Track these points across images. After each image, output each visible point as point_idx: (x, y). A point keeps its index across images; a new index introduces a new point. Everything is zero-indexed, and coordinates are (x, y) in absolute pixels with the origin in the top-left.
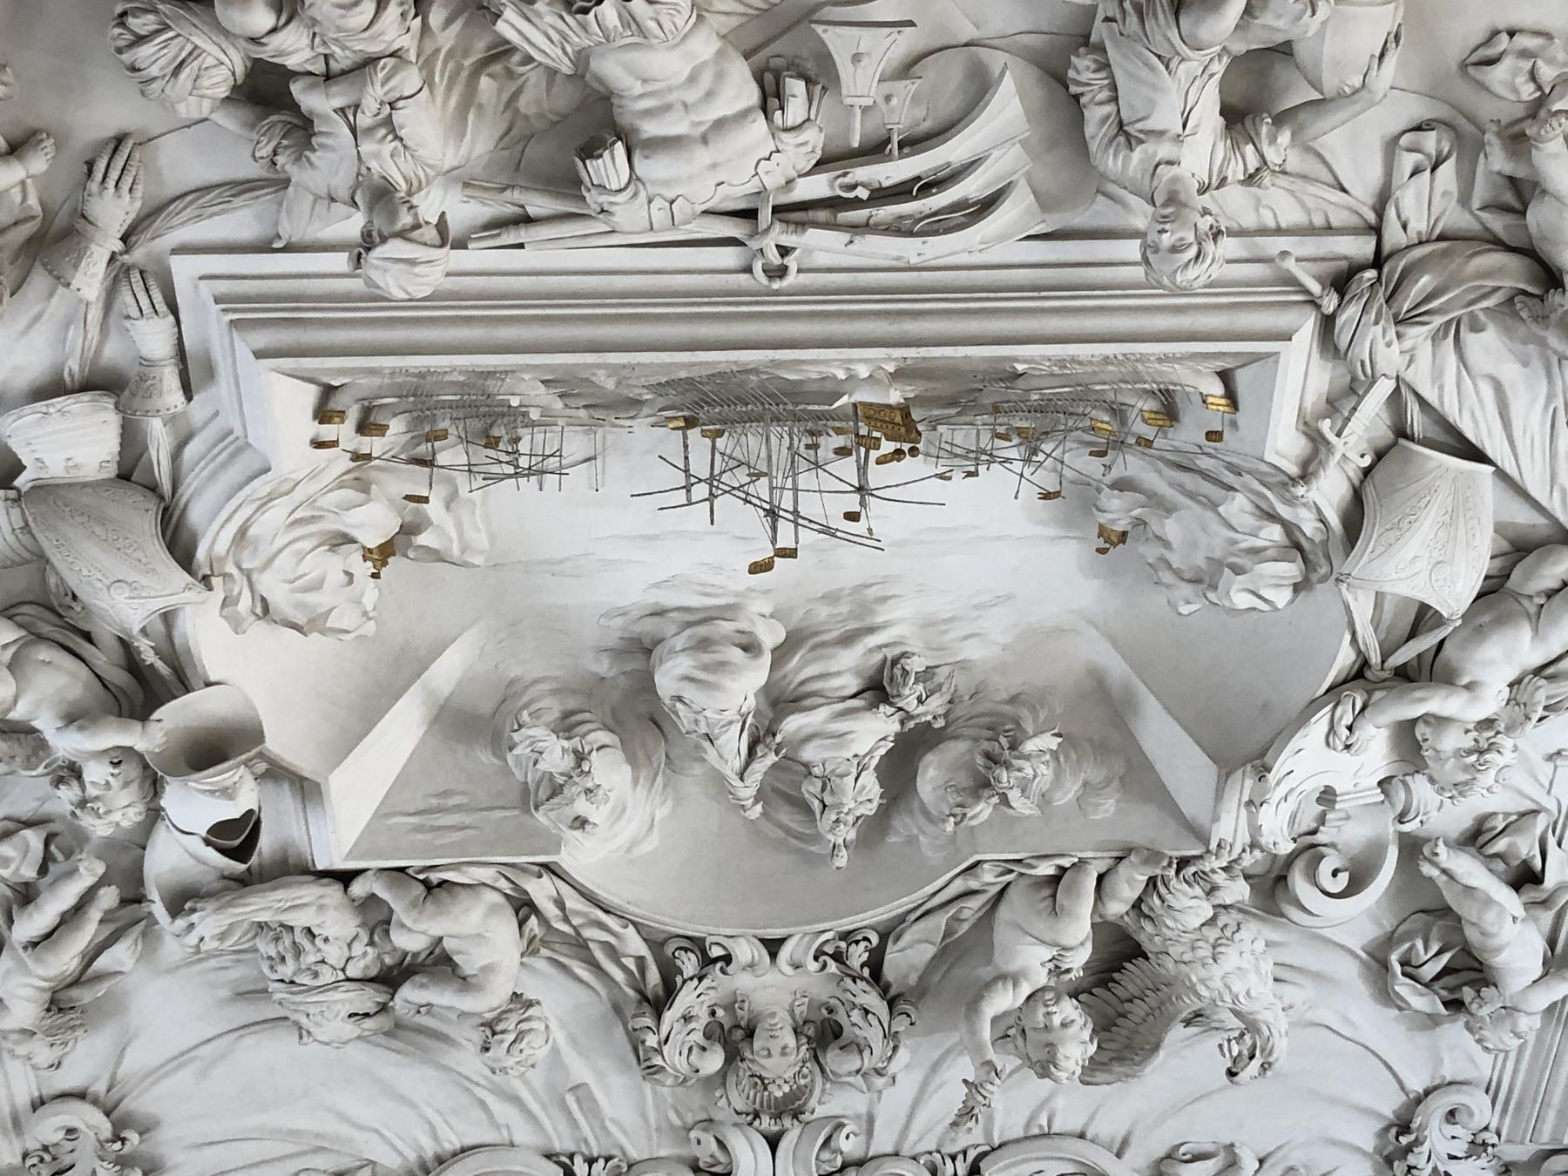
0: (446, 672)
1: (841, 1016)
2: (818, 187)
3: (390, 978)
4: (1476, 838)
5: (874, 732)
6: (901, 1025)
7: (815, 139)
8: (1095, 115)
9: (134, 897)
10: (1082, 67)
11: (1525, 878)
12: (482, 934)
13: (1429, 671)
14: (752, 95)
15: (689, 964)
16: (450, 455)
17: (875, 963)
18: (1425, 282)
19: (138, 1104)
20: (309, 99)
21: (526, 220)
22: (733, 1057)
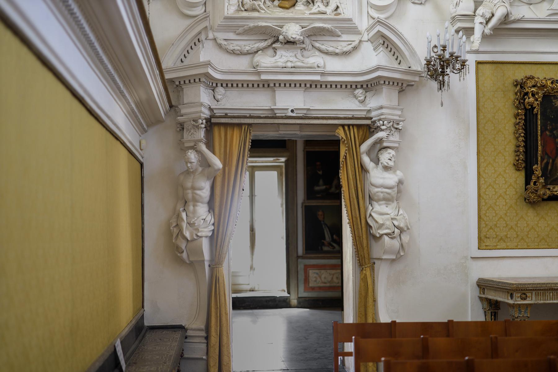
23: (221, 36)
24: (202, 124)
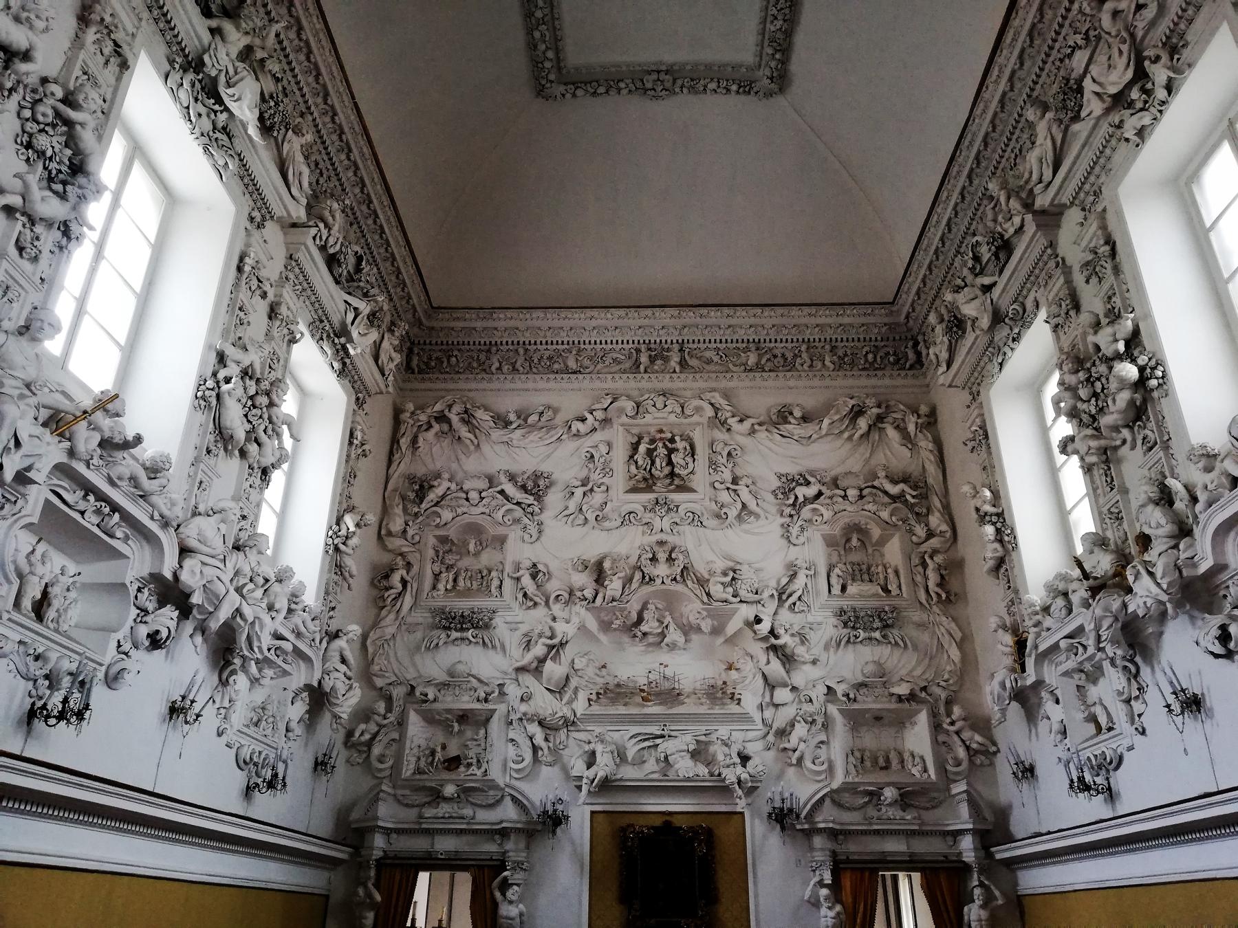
0: (721, 640)
2: (658, 741)
3: (733, 579)
4: (536, 604)
5: (644, 627)
7: (659, 750)
9: (780, 598)
10: (618, 760)
11: (525, 595)
12: (716, 590)
13: (551, 647)
15: (678, 578)
17: (644, 577)
19: (784, 542)
23: (399, 792)
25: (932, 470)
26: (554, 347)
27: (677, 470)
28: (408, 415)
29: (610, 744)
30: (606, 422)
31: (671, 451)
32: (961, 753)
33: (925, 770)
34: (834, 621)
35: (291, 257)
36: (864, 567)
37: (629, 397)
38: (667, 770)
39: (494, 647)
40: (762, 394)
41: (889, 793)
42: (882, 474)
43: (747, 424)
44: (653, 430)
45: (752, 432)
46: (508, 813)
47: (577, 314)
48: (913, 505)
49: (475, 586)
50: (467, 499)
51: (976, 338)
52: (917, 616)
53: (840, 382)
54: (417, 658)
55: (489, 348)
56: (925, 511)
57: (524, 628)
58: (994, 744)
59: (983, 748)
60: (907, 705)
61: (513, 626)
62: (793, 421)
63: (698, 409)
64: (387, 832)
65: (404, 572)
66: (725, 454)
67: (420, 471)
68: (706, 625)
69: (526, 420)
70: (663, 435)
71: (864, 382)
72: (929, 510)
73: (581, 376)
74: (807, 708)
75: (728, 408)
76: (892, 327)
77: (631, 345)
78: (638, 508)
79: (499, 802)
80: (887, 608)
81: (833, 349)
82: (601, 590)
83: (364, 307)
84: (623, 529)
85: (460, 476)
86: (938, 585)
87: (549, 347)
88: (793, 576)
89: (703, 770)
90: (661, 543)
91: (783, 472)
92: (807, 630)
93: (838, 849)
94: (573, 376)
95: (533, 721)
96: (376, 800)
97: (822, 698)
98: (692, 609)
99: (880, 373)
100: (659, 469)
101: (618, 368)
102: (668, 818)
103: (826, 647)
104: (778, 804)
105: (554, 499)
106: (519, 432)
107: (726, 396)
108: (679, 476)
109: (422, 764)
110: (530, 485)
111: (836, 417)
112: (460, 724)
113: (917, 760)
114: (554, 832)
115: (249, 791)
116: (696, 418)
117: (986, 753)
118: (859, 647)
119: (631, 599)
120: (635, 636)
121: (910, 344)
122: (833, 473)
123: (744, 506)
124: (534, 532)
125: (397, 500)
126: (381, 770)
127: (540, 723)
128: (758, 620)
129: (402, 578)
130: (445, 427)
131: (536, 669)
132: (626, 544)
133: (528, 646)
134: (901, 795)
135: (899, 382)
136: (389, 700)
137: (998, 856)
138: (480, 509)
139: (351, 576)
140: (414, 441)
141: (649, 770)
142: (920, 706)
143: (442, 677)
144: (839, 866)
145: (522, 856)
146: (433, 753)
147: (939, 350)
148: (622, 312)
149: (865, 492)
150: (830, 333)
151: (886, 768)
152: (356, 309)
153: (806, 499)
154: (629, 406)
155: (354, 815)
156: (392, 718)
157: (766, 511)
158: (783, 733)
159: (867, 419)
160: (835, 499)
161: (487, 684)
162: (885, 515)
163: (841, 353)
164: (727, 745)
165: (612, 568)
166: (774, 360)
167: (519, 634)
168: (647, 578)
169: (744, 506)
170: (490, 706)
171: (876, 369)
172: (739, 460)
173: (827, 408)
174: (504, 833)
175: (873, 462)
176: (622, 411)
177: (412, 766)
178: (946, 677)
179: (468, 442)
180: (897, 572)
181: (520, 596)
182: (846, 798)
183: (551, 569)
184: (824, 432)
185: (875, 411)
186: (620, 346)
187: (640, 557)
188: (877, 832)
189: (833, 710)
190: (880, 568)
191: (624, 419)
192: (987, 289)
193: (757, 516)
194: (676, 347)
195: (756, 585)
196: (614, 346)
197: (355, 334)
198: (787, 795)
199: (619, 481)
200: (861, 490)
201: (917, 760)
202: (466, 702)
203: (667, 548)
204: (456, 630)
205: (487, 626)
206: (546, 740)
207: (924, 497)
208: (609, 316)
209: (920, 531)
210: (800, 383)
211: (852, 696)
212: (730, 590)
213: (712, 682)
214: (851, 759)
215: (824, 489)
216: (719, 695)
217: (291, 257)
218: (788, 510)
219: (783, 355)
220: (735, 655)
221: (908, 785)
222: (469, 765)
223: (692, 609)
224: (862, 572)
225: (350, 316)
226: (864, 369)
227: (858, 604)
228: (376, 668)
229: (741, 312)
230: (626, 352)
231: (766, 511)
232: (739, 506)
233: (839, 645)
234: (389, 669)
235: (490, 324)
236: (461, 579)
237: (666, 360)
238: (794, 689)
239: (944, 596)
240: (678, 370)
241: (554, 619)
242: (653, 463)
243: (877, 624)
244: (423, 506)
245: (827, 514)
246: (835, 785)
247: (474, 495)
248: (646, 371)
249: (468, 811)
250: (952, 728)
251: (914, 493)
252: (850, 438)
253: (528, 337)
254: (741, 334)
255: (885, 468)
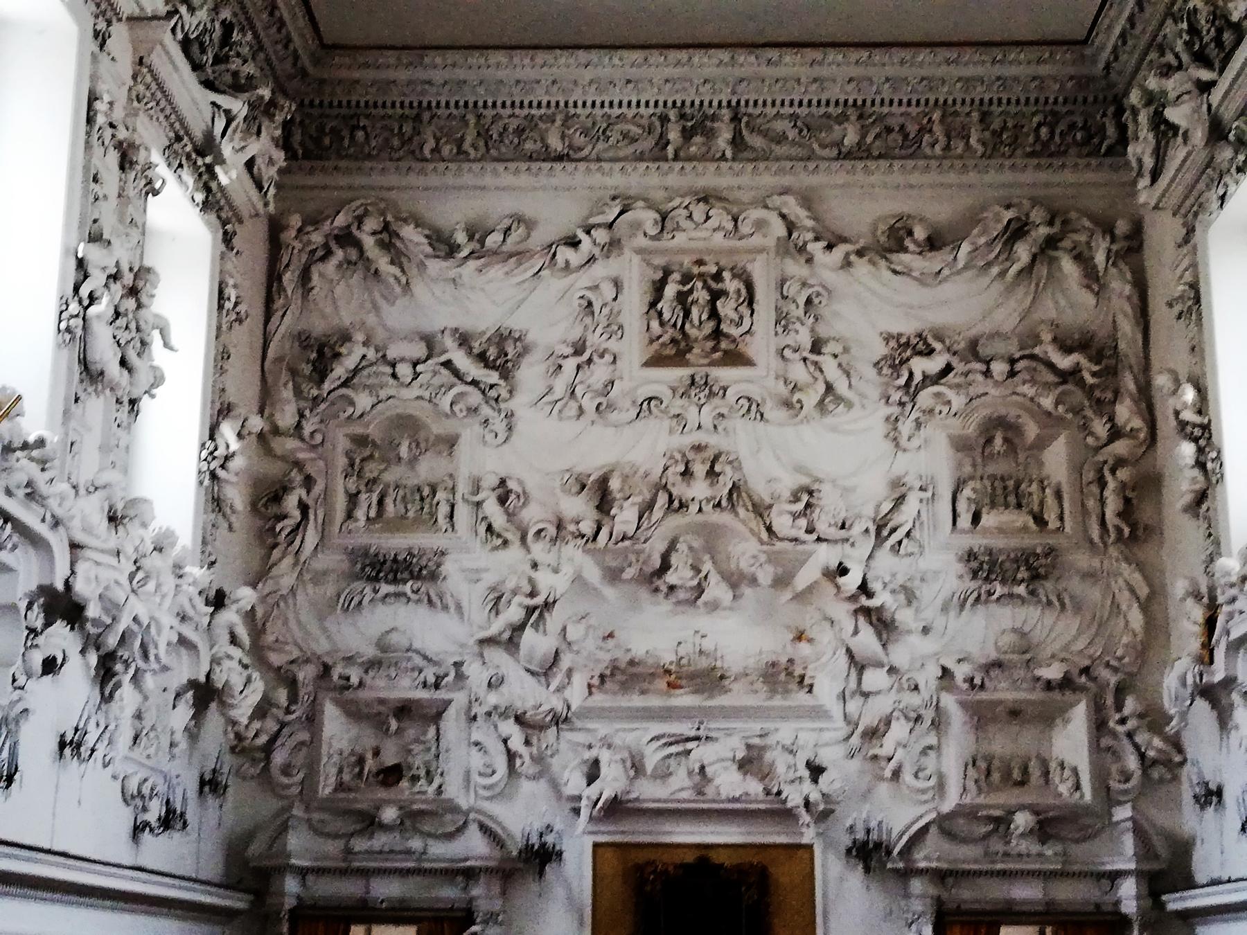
0: (787, 595)
1: (679, 478)
2: (690, 745)
3: (808, 505)
5: (671, 578)
6: (664, 481)
8: (629, 764)
10: (632, 773)
11: (490, 528)
12: (782, 523)
13: (530, 610)
14: (707, 769)
15: (724, 503)
16: (783, 660)
17: (671, 501)
18: (549, 718)
19: (888, 446)
20: (806, 773)
21: (761, 736)
22: (712, 467)
23: (316, 816)
24: (284, 915)
25: (1127, 328)
26: (526, 111)
27: (724, 327)
28: (293, 233)
29: (621, 746)
30: (614, 246)
31: (716, 295)
32: (1132, 763)
33: (1078, 787)
34: (960, 568)
35: (141, 61)
36: (1011, 483)
37: (650, 205)
38: (702, 787)
39: (445, 608)
40: (866, 198)
41: (1022, 820)
42: (1047, 337)
43: (840, 251)
44: (687, 261)
45: (847, 264)
46: (473, 846)
47: (564, 58)
48: (1092, 387)
49: (411, 514)
50: (394, 376)
51: (1189, 154)
52: (1083, 560)
53: (992, 177)
54: (330, 624)
55: (418, 114)
56: (1109, 395)
57: (489, 579)
58: (1180, 750)
59: (1163, 757)
60: (1056, 695)
61: (475, 577)
62: (912, 247)
63: (760, 225)
64: (303, 873)
65: (303, 492)
66: (801, 301)
67: (318, 327)
68: (765, 576)
69: (482, 242)
70: (703, 269)
71: (1028, 177)
72: (1117, 393)
73: (570, 166)
74: (914, 700)
75: (810, 223)
76: (1083, 82)
77: (651, 110)
78: (665, 393)
79: (460, 830)
80: (1038, 551)
81: (985, 117)
82: (606, 520)
83: (238, 106)
84: (639, 424)
85: (380, 335)
86: (1119, 515)
87: (517, 111)
88: (900, 501)
89: (754, 787)
90: (698, 448)
91: (895, 330)
92: (917, 583)
93: (945, 895)
94: (558, 166)
95: (507, 717)
96: (284, 828)
97: (933, 683)
98: (745, 549)
99: (1057, 162)
100: (697, 326)
101: (630, 150)
102: (703, 852)
103: (945, 609)
104: (860, 835)
105: (530, 374)
106: (472, 264)
107: (807, 201)
108: (727, 336)
109: (346, 777)
110: (492, 353)
111: (982, 240)
112: (399, 719)
113: (1067, 773)
114: (541, 873)
115: (138, 829)
116: (757, 240)
117: (1167, 763)
118: (993, 607)
119: (650, 531)
120: (657, 590)
121: (1111, 109)
122: (973, 332)
123: (829, 388)
124: (499, 425)
125: (285, 376)
126: (288, 787)
127: (519, 720)
128: (843, 571)
129: (300, 501)
130: (353, 254)
131: (511, 641)
132: (642, 448)
133: (496, 608)
134: (1039, 822)
135: (1090, 176)
136: (292, 684)
137: (1172, 906)
138: (414, 391)
139: (234, 512)
140: (305, 276)
141: (677, 787)
142: (1078, 695)
143: (370, 652)
144: (943, 918)
145: (497, 905)
146: (361, 761)
147: (1141, 149)
148: (637, 55)
149: (1019, 366)
150: (979, 92)
151: (1022, 783)
152: (227, 112)
153: (925, 377)
154: (648, 218)
155: (255, 848)
156: (299, 711)
157: (862, 396)
158: (873, 734)
159: (1035, 240)
160: (971, 377)
161: (436, 663)
162: (1047, 402)
163: (996, 124)
164: (791, 752)
165: (621, 490)
166: (889, 138)
167: (481, 588)
168: (676, 504)
169: (829, 388)
170: (442, 695)
171: (1051, 155)
172: (824, 311)
173: (973, 219)
174: (470, 874)
175: (1037, 315)
176: (636, 226)
177: (332, 780)
178: (1119, 653)
179: (392, 280)
180: (1058, 495)
181: (482, 528)
182: (961, 824)
183: (530, 487)
184: (961, 264)
185: (1043, 231)
186: (634, 110)
187: (666, 469)
188: (1003, 874)
189: (949, 701)
190: (1034, 487)
191: (641, 241)
192: (1205, 87)
193: (849, 405)
194: (726, 114)
195: (843, 515)
196: (624, 109)
197: (227, 149)
198: (873, 824)
199: (632, 347)
200: (1012, 362)
201: (1067, 773)
202: (406, 689)
203: (710, 454)
204: (387, 582)
205: (434, 576)
206: (527, 743)
207: (1110, 373)
208: (616, 61)
209: (1100, 428)
210: (927, 178)
211: (977, 681)
212: (803, 522)
213: (774, 658)
214: (972, 772)
215: (955, 362)
216: (782, 677)
217: (141, 61)
218: (896, 396)
219: (902, 127)
220: (808, 618)
221: (1050, 808)
222: (415, 779)
223: (745, 549)
224: (1007, 493)
225: (220, 124)
226: (1032, 154)
227: (999, 543)
228: (270, 638)
229: (833, 55)
230: (645, 122)
231: (862, 396)
232: (821, 388)
233: (962, 606)
234: (290, 640)
235: (421, 74)
236: (389, 501)
237: (710, 134)
238: (892, 670)
239: (1127, 531)
240: (729, 154)
241: (535, 566)
242: (687, 314)
243: (1023, 574)
244: (327, 386)
245: (958, 401)
246: (947, 806)
247: (404, 370)
248: (676, 158)
249: (416, 844)
250: (1121, 729)
251: (1096, 368)
252: (1002, 274)
253: (482, 94)
254: (835, 92)
255: (1054, 325)
